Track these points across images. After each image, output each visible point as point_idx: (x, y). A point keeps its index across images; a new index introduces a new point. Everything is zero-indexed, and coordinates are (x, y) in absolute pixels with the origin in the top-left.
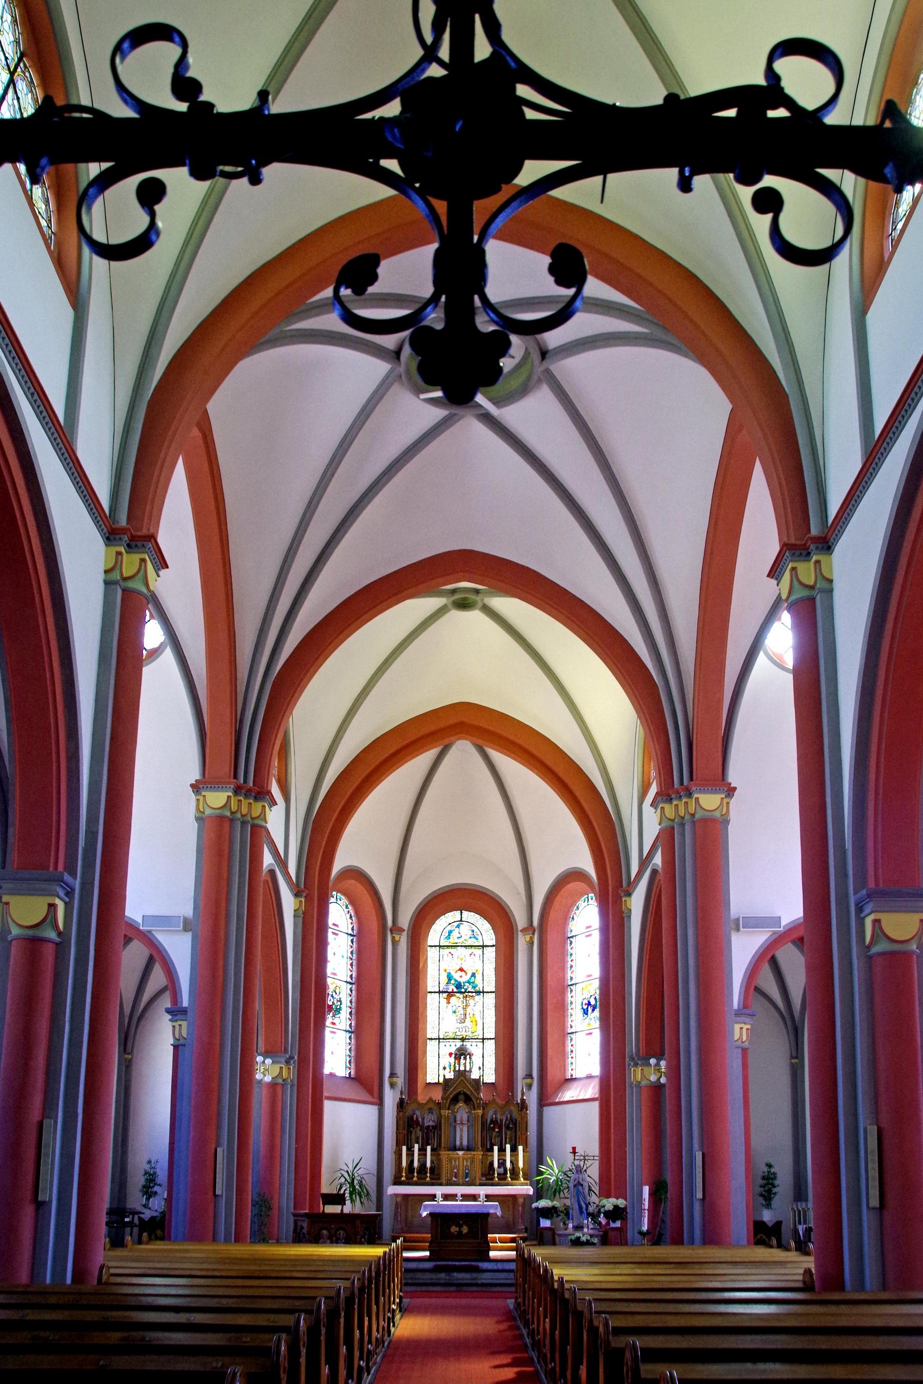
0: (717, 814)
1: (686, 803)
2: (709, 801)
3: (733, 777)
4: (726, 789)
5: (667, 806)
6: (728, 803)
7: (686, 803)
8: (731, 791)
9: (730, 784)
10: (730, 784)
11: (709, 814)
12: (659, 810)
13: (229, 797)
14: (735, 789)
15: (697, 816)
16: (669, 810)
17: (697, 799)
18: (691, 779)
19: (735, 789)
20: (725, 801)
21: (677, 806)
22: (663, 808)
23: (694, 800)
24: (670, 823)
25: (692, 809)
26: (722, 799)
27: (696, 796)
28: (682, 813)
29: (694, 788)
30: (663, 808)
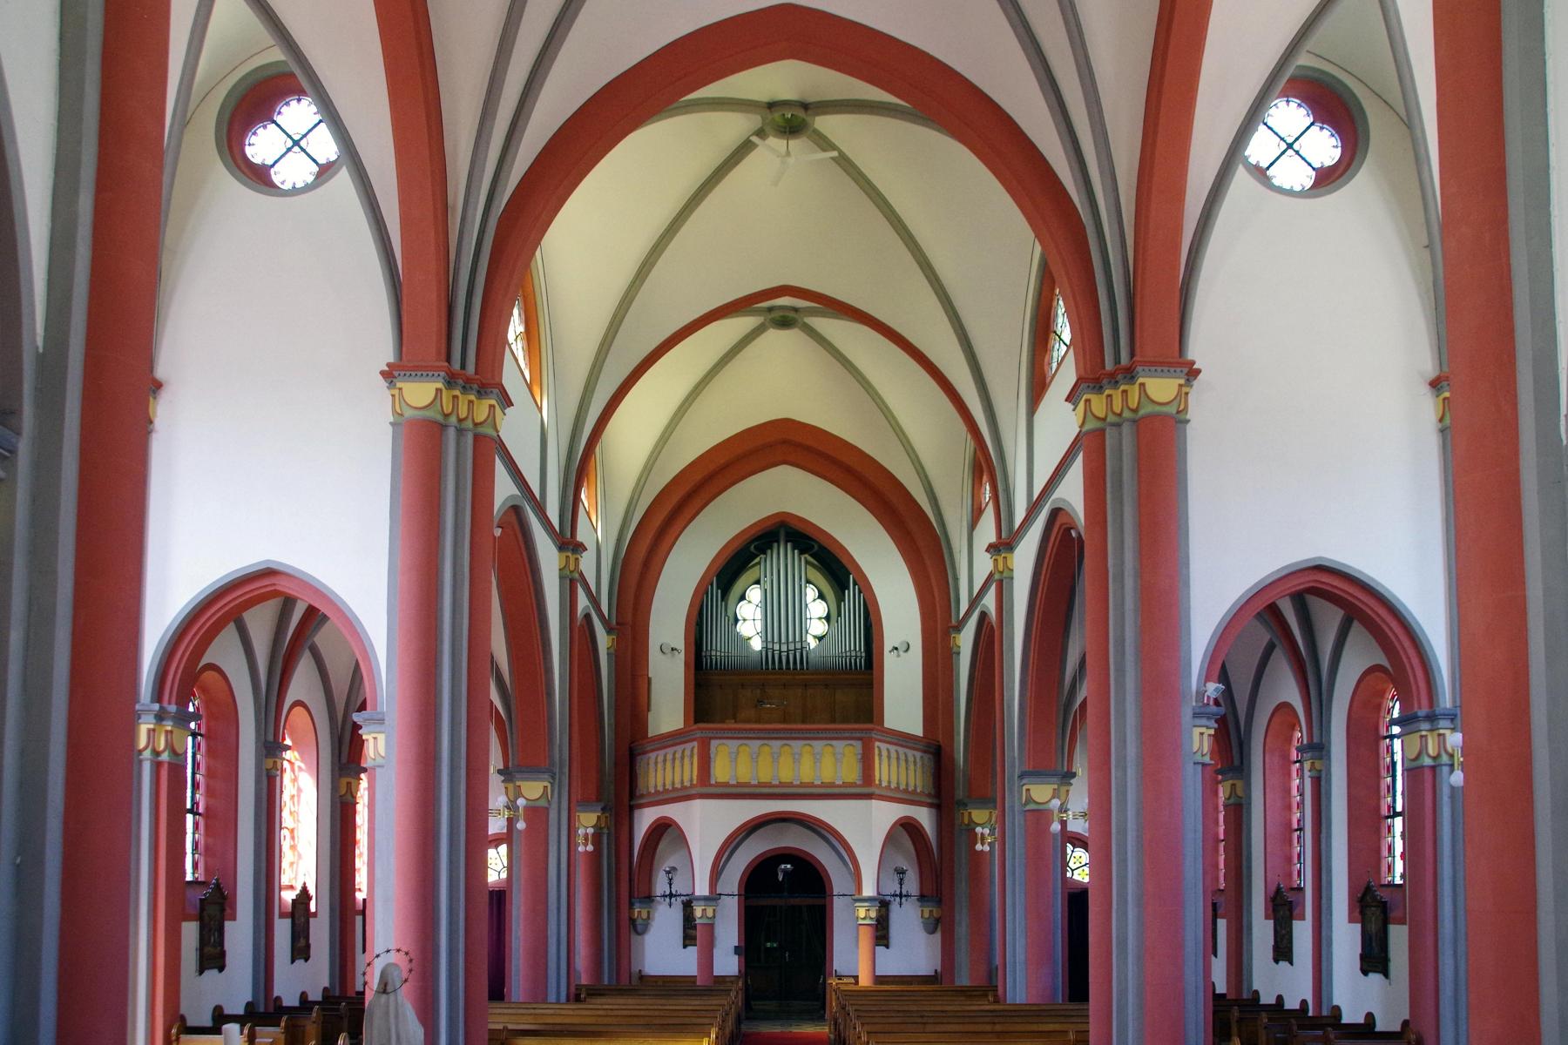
0: (1172, 410)
1: (1125, 392)
2: (1161, 388)
3: (1196, 351)
4: (1186, 370)
5: (1094, 398)
6: (1187, 394)
7: (1125, 392)
8: (1192, 373)
9: (1193, 363)
10: (1193, 363)
11: (1158, 409)
12: (1081, 405)
13: (437, 390)
14: (1198, 372)
15: (1142, 412)
16: (1098, 404)
17: (1142, 385)
18: (1132, 354)
19: (1198, 372)
20: (1185, 389)
21: (1109, 396)
22: (1088, 401)
23: (1137, 386)
24: (1099, 425)
25: (1133, 403)
26: (1180, 386)
27: (1141, 380)
28: (1117, 408)
29: (1139, 369)
30: (1088, 401)
